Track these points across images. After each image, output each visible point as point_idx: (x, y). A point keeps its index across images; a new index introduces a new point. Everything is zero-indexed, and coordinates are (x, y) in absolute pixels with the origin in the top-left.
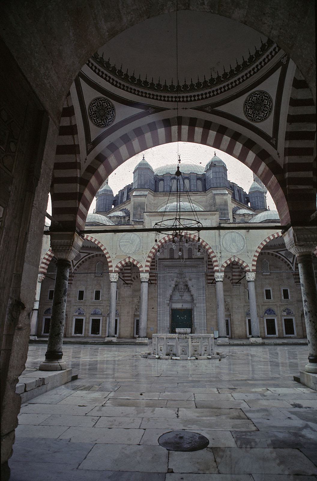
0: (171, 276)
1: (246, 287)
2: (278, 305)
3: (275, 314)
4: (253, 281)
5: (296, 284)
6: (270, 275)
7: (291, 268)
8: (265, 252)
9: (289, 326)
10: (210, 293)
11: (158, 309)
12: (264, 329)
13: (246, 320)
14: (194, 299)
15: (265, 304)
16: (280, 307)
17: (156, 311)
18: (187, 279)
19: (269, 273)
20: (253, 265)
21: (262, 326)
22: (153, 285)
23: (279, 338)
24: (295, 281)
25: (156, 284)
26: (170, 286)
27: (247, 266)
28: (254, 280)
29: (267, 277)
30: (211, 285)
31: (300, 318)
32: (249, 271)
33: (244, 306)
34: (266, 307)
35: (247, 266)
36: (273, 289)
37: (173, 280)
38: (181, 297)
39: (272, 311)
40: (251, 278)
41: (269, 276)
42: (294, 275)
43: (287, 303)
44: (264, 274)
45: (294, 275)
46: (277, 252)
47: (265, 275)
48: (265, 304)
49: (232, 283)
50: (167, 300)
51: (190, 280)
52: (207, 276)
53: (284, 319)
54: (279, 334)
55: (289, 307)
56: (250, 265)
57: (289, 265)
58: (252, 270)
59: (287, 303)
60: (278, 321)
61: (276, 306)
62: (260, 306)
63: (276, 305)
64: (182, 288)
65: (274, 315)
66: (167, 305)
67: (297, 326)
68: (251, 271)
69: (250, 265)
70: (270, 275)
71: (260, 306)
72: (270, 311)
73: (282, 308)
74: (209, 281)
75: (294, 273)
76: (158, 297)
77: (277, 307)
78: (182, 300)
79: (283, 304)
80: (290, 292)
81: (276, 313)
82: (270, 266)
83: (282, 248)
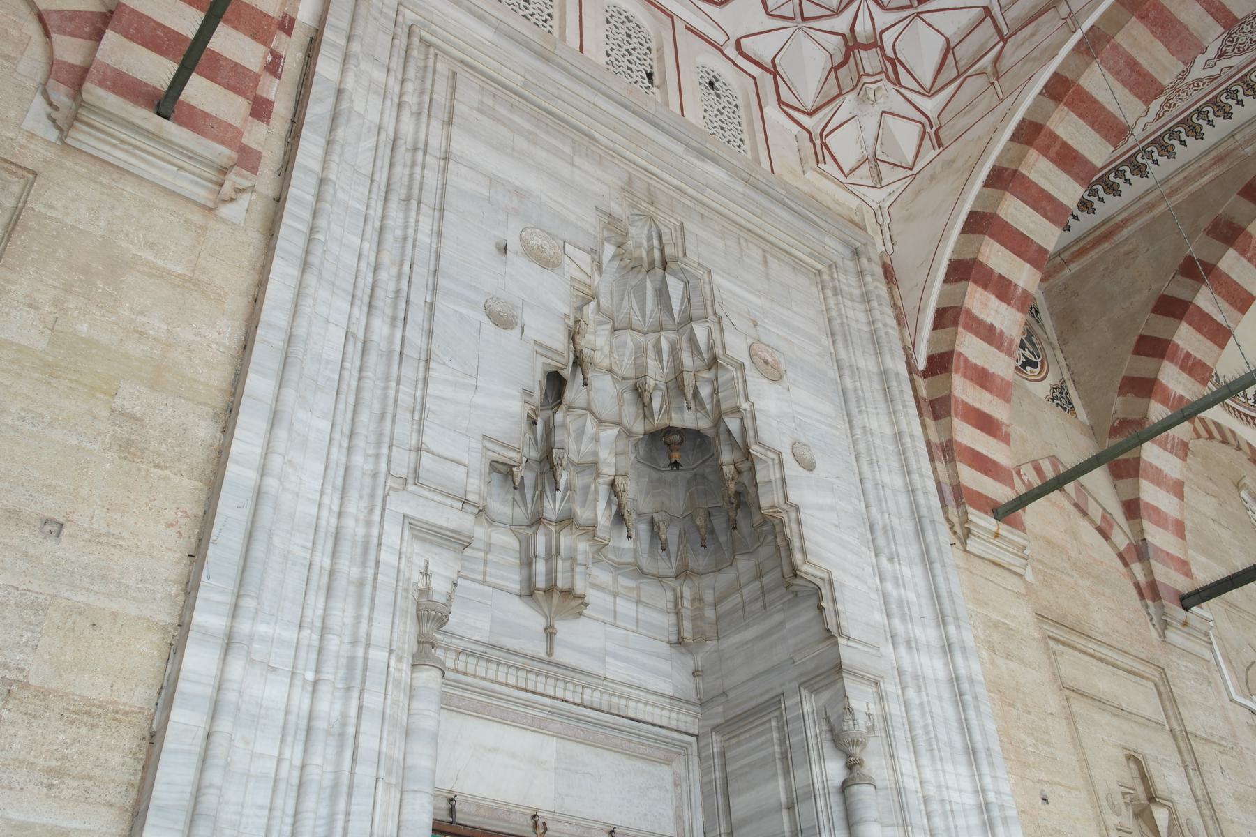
0: (520, 193)
10: (996, 626)
11: (199, 661)
14: (849, 654)
17: (88, 714)
18: (736, 346)
22: (171, 129)
25: (248, 159)
26: (503, 320)
30: (989, 522)
37: (548, 263)
38: (530, 618)
49: (1150, 591)
50: (421, 531)
51: (774, 373)
52: (937, 408)
64: (592, 467)
66: (407, 632)
74: (969, 477)
76: (258, 384)
78: (549, 664)
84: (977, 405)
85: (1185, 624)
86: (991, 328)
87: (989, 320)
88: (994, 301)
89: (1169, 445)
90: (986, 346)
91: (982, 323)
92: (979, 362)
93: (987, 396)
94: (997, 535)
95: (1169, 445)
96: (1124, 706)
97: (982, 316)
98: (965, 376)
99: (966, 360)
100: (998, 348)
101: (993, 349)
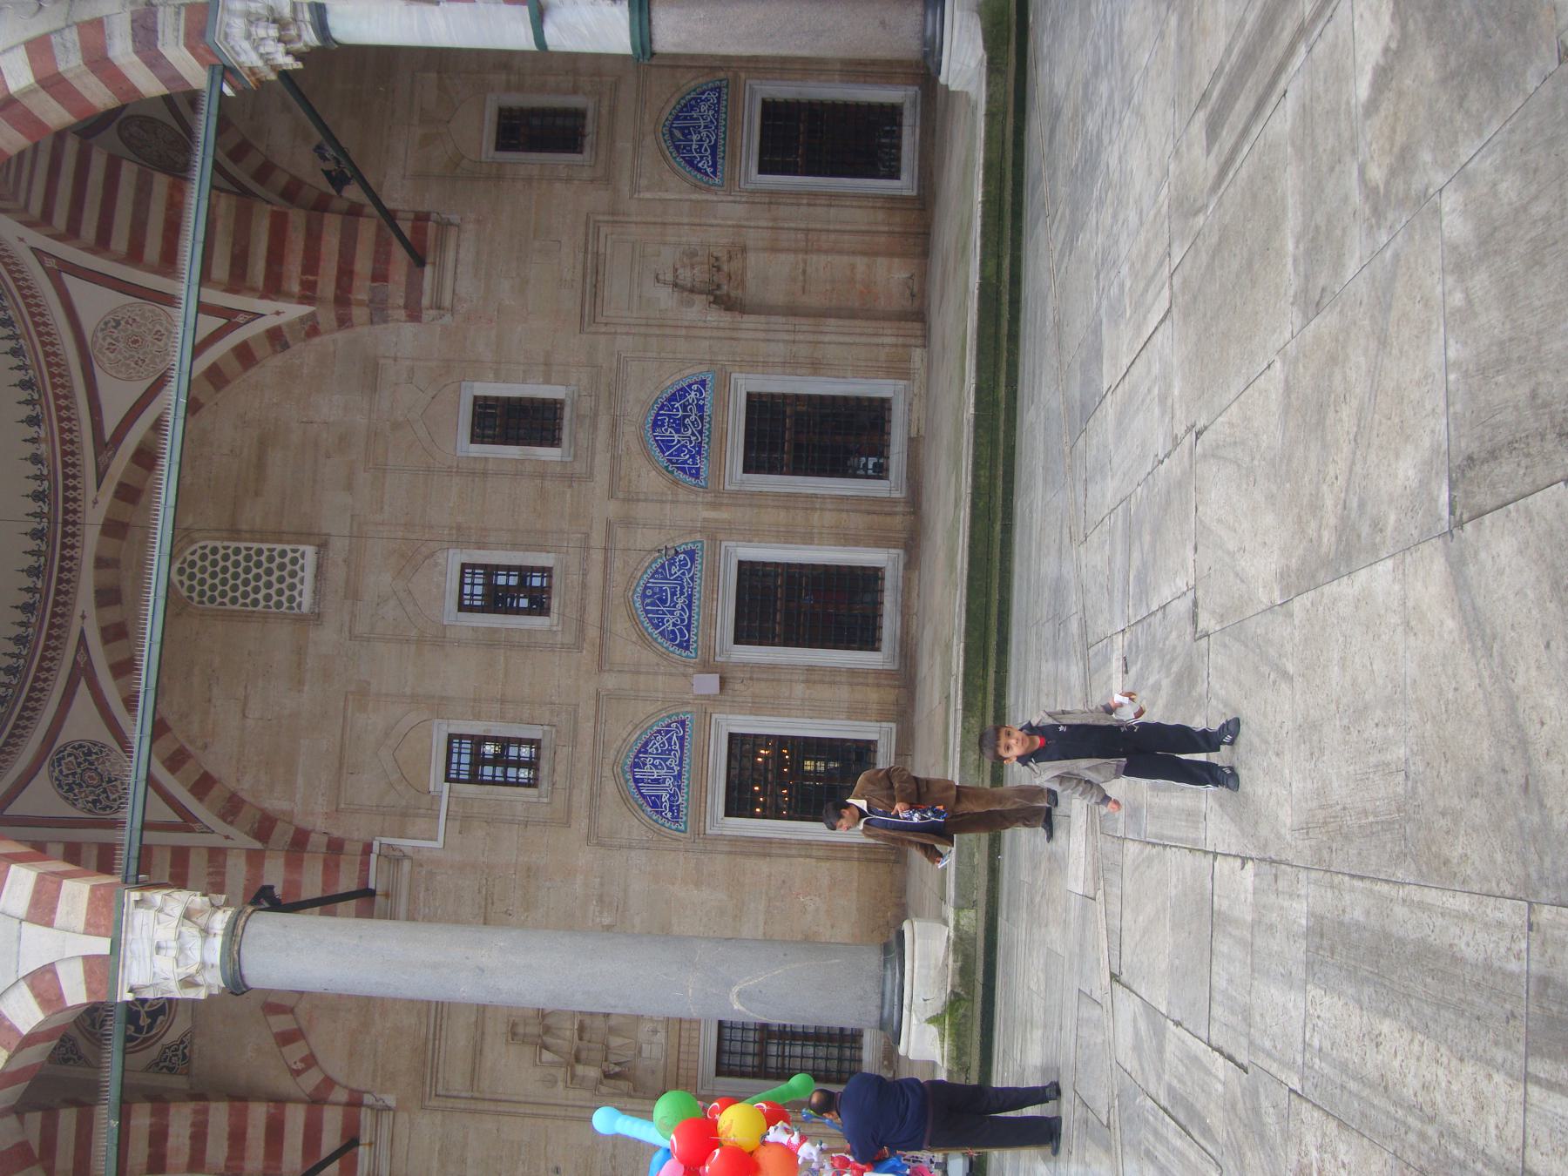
1: (288, 1015)
2: (613, 509)
3: (691, 554)
4: (233, 934)
5: (428, 315)
6: (322, 546)
7: (276, 336)
8: (100, 563)
9: (818, 437)
12: (830, 676)
13: (734, 840)
15: (592, 633)
16: (631, 499)
19: (310, 551)
20: (43, 910)
21: (799, 690)
23: (912, 544)
24: (402, 314)
27: (43, 982)
28: (220, 921)
29: (337, 574)
31: (749, 321)
32: (102, 969)
33: (594, 838)
34: (621, 626)
35: (43, 982)
36: (461, 537)
39: (660, 572)
40: (195, 955)
41: (339, 546)
42: (344, 322)
43: (604, 422)
44: (306, 601)
45: (344, 322)
46: (105, 446)
47: (316, 591)
48: (592, 633)
53: (746, 471)
54: (879, 542)
55: (640, 399)
56: (39, 947)
57: (244, 354)
58: (92, 928)
59: (604, 422)
60: (753, 534)
61: (620, 532)
62: (610, 681)
63: (609, 523)
65: (700, 568)
67: (816, 367)
68: (101, 946)
69: (39, 947)
70: (322, 546)
71: (610, 681)
72: (665, 604)
73: (649, 477)
75: (327, 316)
77: (628, 522)
79: (602, 461)
80: (497, 379)
81: (683, 542)
82: (234, 533)
83: (69, 396)
84: (262, 1144)
85: (387, 895)
86: (193, 1137)
87: (187, 1142)
88: (172, 1142)
89: (218, 879)
90: (210, 1138)
91: (192, 1148)
92: (225, 1144)
93: (251, 1132)
94: (370, 1144)
95: (218, 879)
96: (473, 1019)
97: (187, 1150)
98: (242, 1158)
99: (229, 1159)
100: (206, 1126)
101: (210, 1130)
